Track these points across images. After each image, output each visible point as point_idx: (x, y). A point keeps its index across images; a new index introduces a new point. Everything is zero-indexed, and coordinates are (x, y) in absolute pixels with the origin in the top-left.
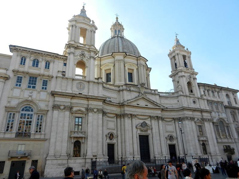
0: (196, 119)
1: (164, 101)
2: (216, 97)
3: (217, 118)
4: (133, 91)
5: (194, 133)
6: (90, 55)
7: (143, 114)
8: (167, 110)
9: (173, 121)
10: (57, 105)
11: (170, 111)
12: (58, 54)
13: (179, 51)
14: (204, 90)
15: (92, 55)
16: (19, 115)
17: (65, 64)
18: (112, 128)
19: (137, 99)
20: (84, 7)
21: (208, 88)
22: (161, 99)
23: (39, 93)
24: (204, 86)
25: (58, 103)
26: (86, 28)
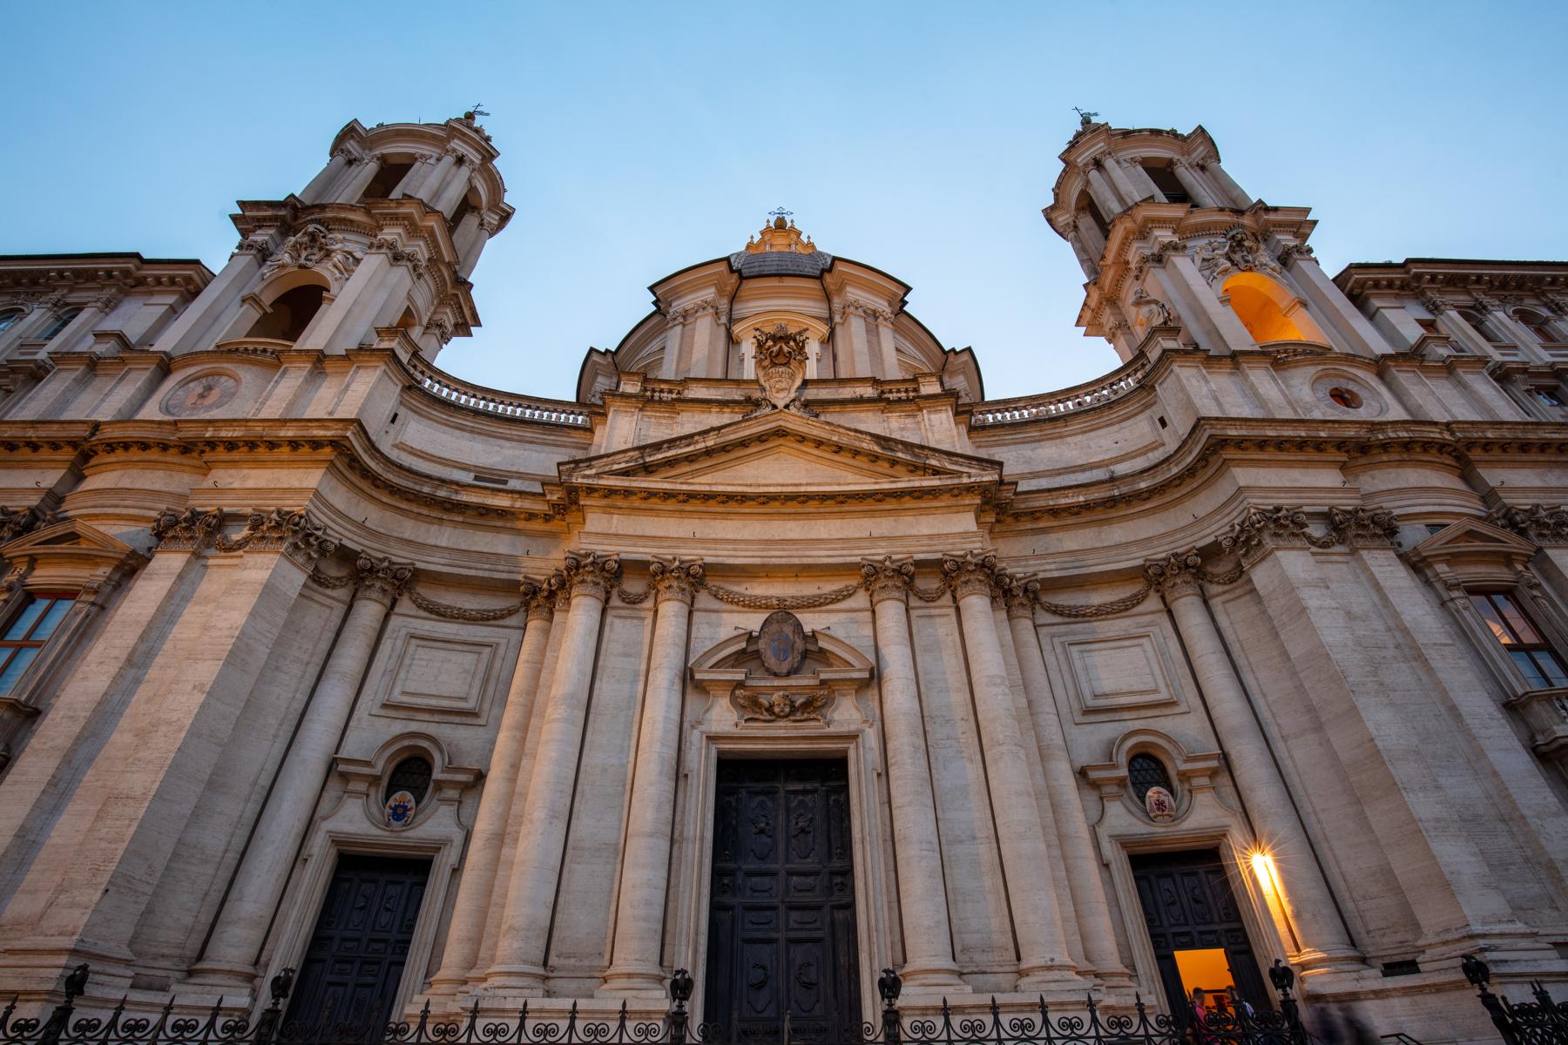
1: (1029, 453)
5: (1430, 671)
7: (777, 556)
8: (1055, 512)
9: (1152, 602)
11: (1099, 514)
12: (137, 256)
14: (1428, 316)
18: (445, 703)
19: (710, 443)
24: (1404, 286)
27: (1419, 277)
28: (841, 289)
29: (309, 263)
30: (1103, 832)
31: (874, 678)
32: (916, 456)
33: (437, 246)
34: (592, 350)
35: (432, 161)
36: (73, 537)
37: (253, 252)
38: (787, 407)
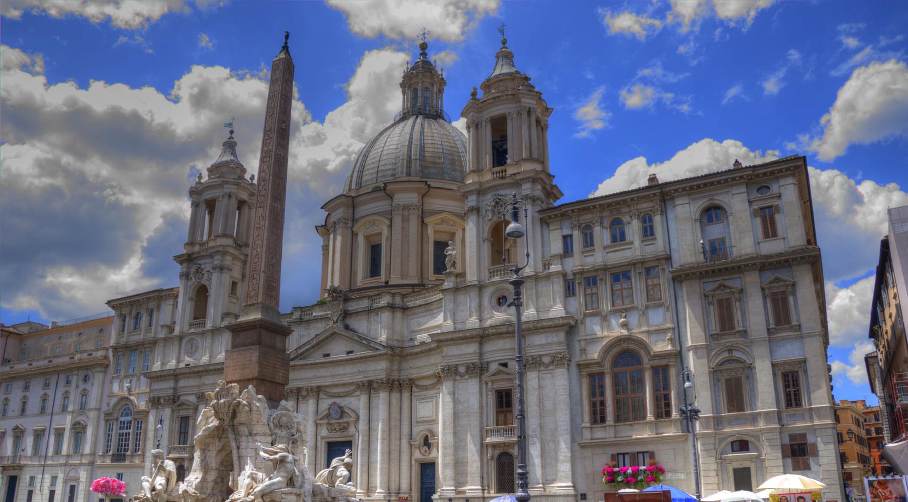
0: (494, 367)
1: (420, 319)
2: (632, 243)
3: (607, 340)
4: (316, 319)
6: (213, 263)
7: (336, 380)
10: (154, 397)
13: (471, 114)
14: (567, 232)
15: (215, 262)
16: (116, 425)
17: (175, 306)
19: (315, 342)
20: (232, 132)
21: (587, 218)
22: (413, 317)
23: (139, 379)
24: (563, 215)
25: (156, 394)
26: (213, 195)
27: (567, 211)
28: (394, 194)
29: (199, 280)
30: (413, 458)
31: (358, 419)
32: (368, 342)
33: (232, 254)
34: (316, 227)
35: (221, 199)
36: (182, 404)
37: (184, 278)
38: (337, 320)
